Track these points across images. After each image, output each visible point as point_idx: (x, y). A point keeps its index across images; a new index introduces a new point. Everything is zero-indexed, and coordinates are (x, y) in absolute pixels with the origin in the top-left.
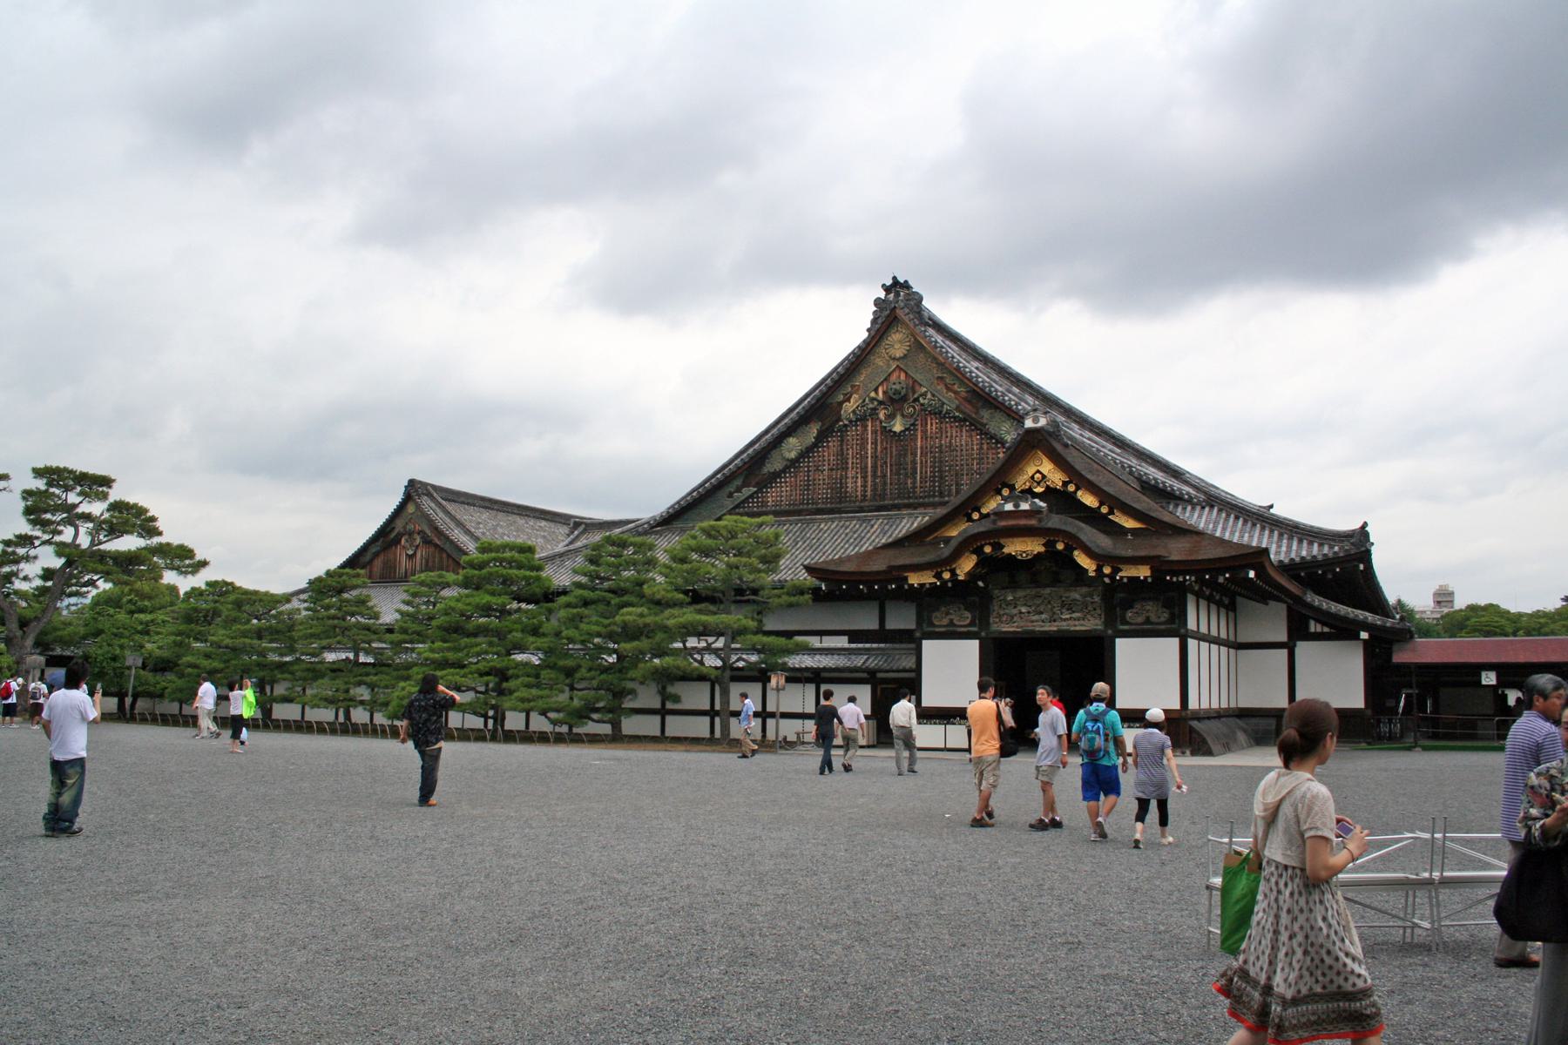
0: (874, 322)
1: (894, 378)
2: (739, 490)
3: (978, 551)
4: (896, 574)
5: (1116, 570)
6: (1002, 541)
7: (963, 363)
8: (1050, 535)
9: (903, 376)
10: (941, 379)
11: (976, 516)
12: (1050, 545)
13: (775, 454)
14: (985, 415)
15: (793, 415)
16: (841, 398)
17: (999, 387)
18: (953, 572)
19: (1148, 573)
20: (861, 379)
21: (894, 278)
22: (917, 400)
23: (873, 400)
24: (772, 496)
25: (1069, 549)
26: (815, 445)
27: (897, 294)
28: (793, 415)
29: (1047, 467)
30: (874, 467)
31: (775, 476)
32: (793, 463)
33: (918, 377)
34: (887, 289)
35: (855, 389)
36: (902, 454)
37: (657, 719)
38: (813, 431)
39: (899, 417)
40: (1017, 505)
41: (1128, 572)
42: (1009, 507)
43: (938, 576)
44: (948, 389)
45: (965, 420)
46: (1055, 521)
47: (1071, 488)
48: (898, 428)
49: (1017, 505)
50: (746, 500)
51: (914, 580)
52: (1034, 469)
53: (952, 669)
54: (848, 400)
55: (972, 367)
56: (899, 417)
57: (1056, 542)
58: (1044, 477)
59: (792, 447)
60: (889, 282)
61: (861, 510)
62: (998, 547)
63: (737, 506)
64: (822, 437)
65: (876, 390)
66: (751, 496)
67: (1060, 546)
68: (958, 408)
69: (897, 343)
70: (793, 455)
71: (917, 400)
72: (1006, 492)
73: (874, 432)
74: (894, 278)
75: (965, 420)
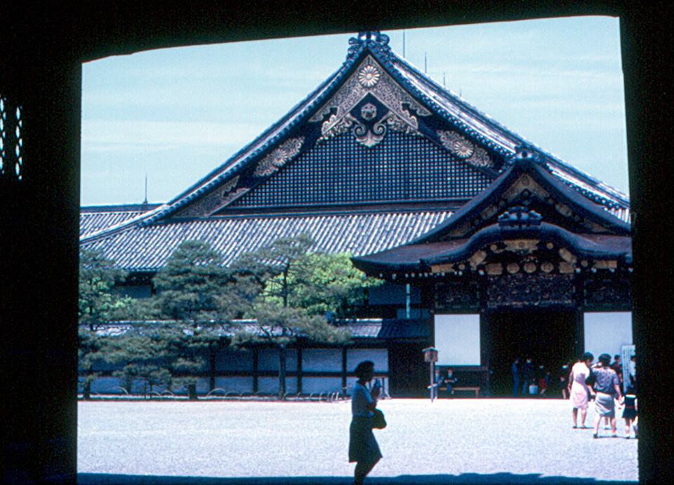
0: (350, 56)
2: (234, 190)
3: (488, 250)
4: (424, 266)
5: (591, 264)
6: (506, 242)
7: (424, 92)
8: (543, 237)
10: (406, 107)
11: (477, 222)
12: (541, 245)
13: (265, 162)
14: (442, 135)
15: (280, 130)
17: (453, 112)
18: (467, 264)
19: (615, 266)
22: (385, 121)
24: (264, 194)
25: (557, 248)
26: (300, 155)
28: (280, 130)
29: (532, 186)
31: (266, 178)
32: (282, 169)
35: (334, 111)
37: (339, 380)
38: (299, 143)
40: (519, 216)
41: (603, 265)
42: (514, 217)
43: (456, 268)
44: (413, 113)
45: (425, 138)
46: (547, 226)
47: (551, 202)
49: (519, 216)
50: (240, 199)
51: (436, 270)
52: (523, 187)
53: (458, 339)
55: (431, 95)
57: (545, 244)
58: (530, 193)
59: (281, 157)
62: (501, 246)
63: (233, 204)
64: (304, 150)
66: (245, 196)
67: (550, 246)
68: (419, 130)
69: (369, 76)
70: (281, 162)
72: (502, 203)
75: (425, 138)
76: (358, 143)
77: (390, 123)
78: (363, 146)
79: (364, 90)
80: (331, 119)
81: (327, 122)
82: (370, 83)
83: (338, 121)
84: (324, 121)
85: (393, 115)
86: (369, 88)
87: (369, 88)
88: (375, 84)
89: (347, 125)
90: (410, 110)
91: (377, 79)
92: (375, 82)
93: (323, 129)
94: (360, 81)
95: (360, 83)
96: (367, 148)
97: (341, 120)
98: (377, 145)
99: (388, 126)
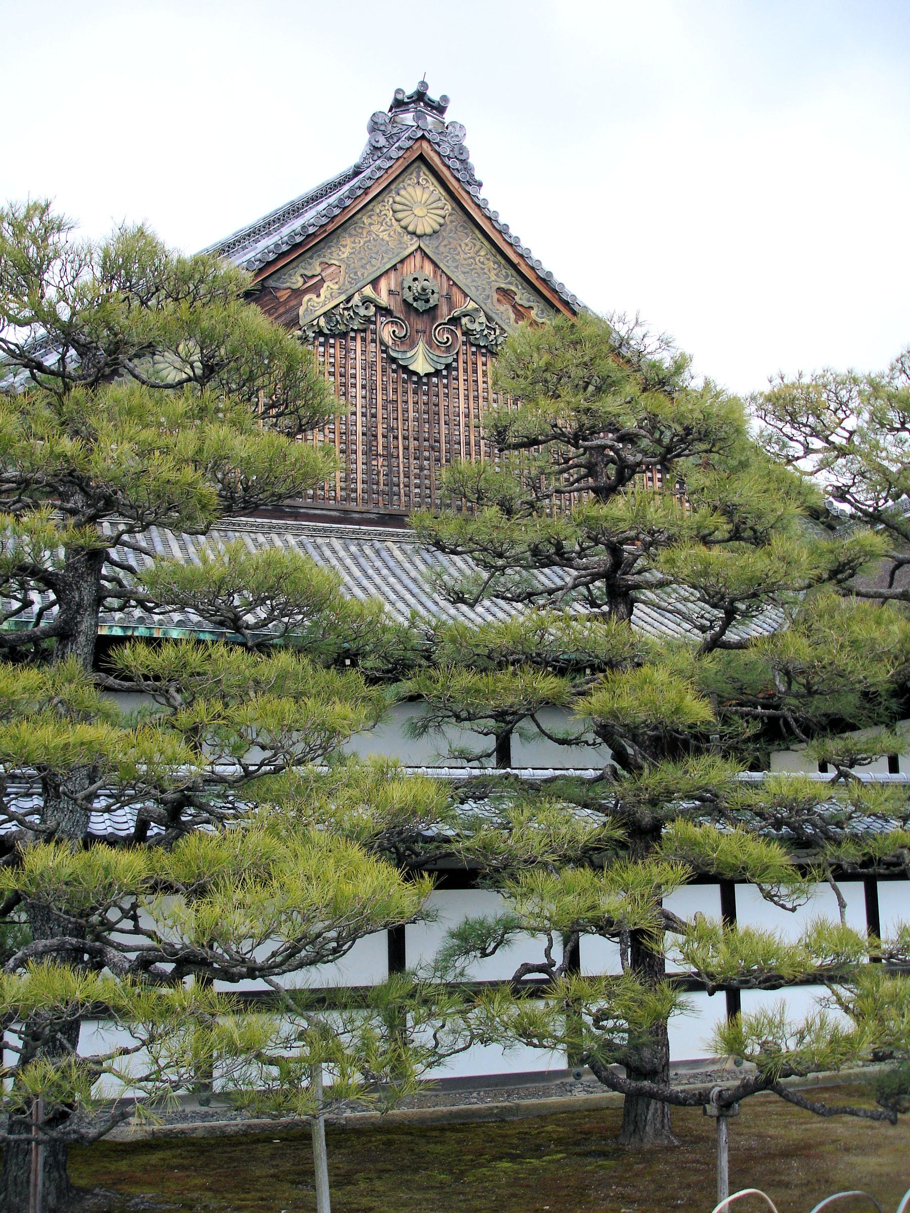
1: (410, 268)
9: (428, 268)
10: (505, 293)
16: (297, 282)
20: (344, 251)
21: (424, 84)
23: (366, 301)
27: (419, 116)
30: (370, 435)
33: (460, 279)
34: (399, 104)
36: (431, 415)
39: (421, 347)
48: (421, 366)
54: (315, 289)
56: (421, 347)
60: (410, 89)
61: (345, 517)
65: (375, 283)
71: (455, 321)
73: (369, 366)
74: (424, 84)
76: (394, 360)
77: (470, 326)
78: (405, 369)
79: (407, 238)
80: (323, 291)
81: (314, 296)
82: (426, 225)
83: (343, 297)
84: (298, 293)
85: (476, 310)
86: (419, 237)
87: (419, 237)
88: (435, 232)
89: (362, 312)
90: (514, 306)
91: (442, 221)
92: (437, 227)
93: (301, 311)
94: (399, 215)
95: (398, 220)
96: (415, 373)
97: (348, 300)
98: (437, 373)
99: (467, 333)
